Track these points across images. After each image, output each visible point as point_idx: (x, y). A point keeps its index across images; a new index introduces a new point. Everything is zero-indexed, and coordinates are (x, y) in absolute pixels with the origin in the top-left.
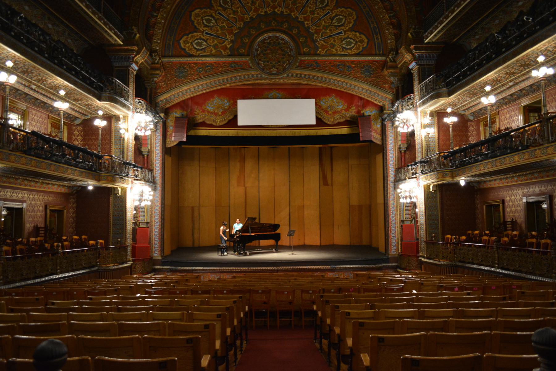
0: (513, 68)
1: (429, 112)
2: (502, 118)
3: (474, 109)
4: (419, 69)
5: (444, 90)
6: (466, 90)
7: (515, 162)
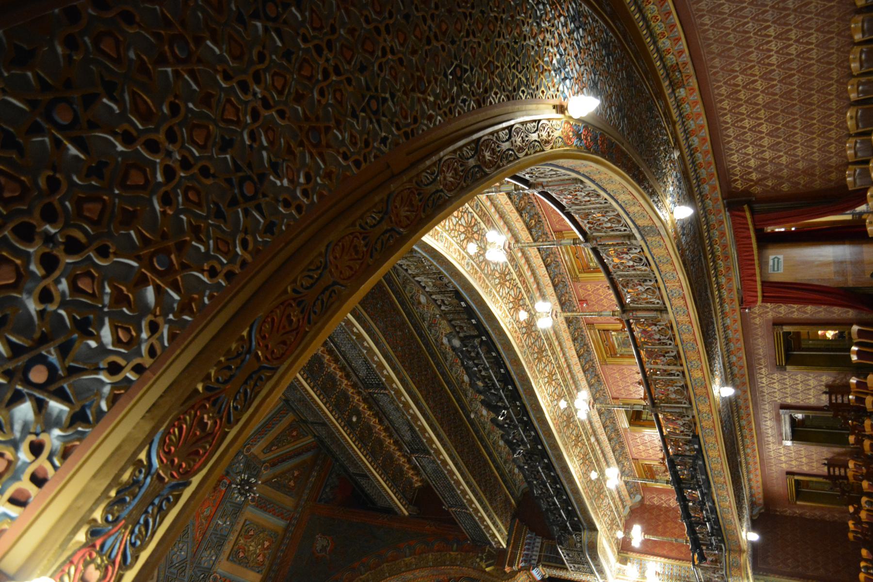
0: (568, 437)
1: (619, 565)
2: (644, 455)
3: (625, 493)
4: (544, 566)
5: (585, 535)
6: (592, 504)
7: (720, 456)
